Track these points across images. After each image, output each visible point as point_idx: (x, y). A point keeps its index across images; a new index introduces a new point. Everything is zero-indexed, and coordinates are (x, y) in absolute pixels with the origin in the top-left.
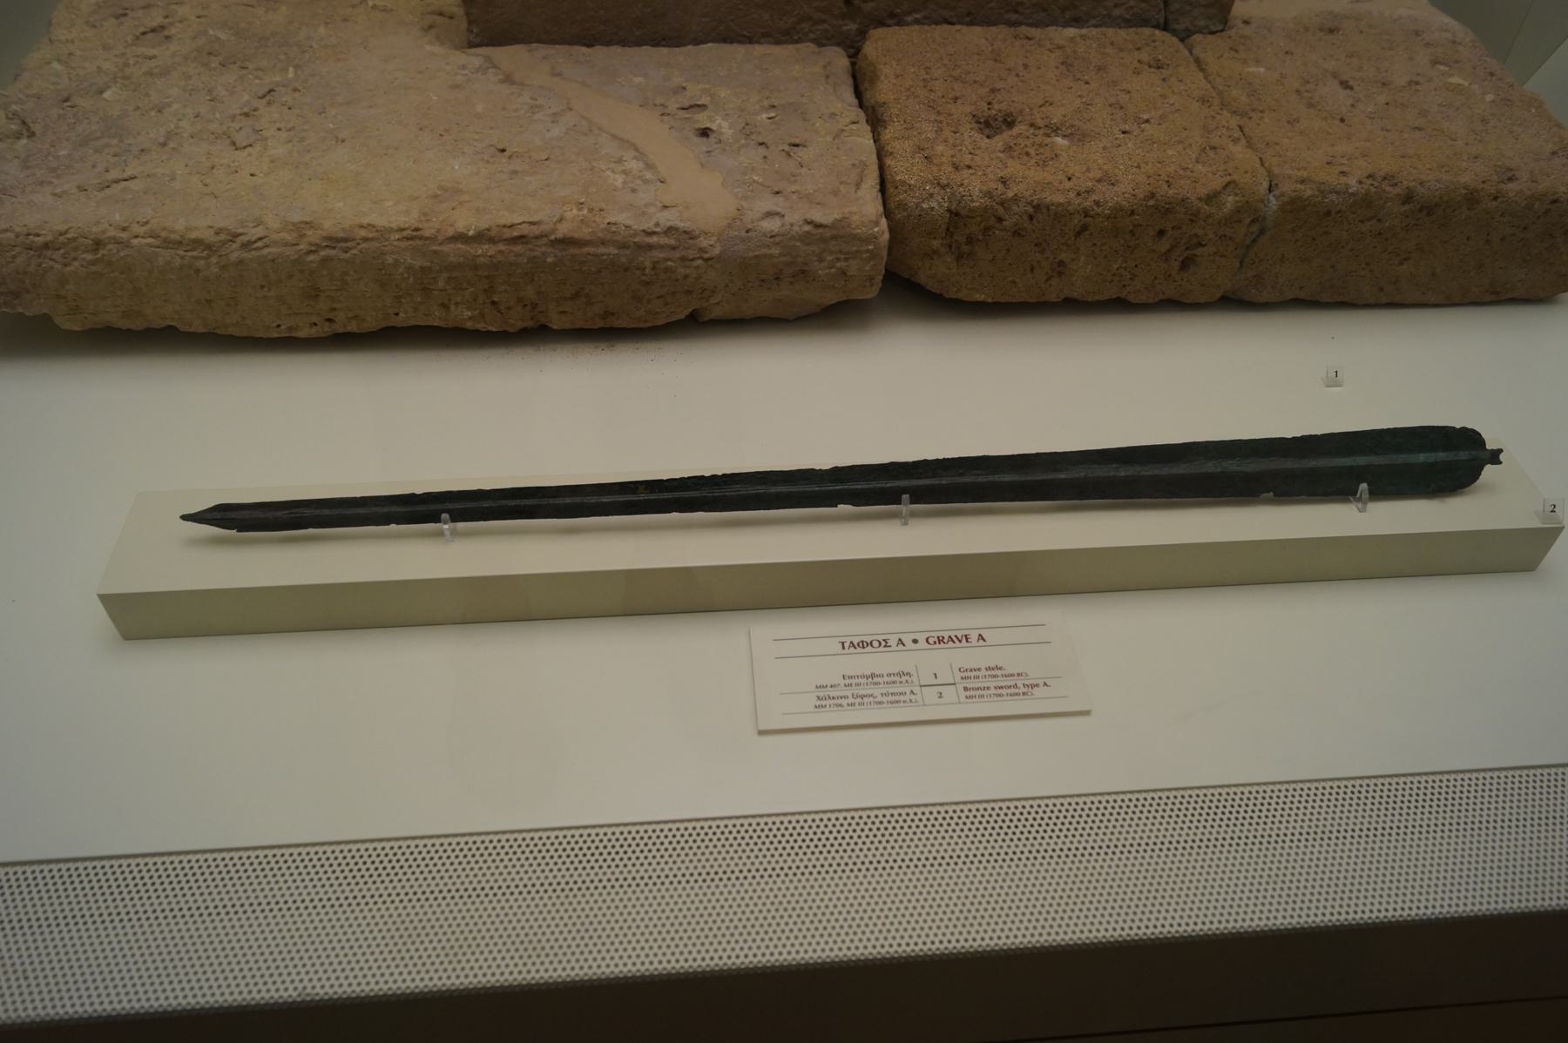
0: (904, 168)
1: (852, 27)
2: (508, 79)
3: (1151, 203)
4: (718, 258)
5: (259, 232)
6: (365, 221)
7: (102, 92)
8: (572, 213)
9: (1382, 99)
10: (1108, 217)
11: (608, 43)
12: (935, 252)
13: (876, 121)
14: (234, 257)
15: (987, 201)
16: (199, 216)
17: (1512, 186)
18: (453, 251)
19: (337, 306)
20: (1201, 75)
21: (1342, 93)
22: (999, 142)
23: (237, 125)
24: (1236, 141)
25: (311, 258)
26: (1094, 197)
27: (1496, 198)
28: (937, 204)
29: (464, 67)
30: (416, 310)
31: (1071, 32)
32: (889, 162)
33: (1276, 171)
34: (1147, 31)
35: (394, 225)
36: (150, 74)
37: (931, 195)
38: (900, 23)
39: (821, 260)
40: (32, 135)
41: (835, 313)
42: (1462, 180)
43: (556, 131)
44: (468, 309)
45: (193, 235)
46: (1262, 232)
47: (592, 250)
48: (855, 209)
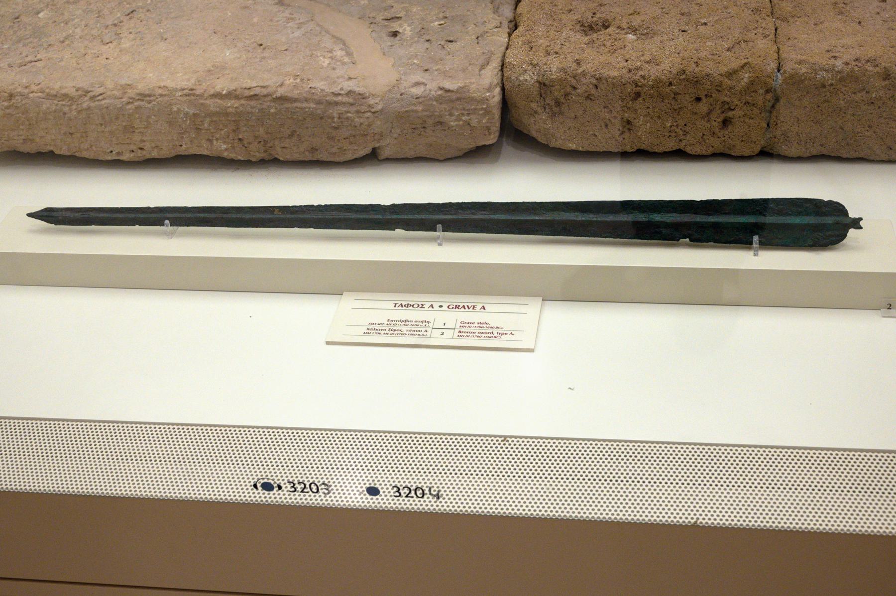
3: (683, 77)
4: (382, 111)
5: (101, 90)
7: (38, 13)
8: (289, 81)
14: (85, 105)
15: (562, 75)
18: (213, 105)
19: (145, 139)
25: (130, 106)
26: (642, 73)
35: (178, 87)
37: (525, 71)
39: (451, 115)
43: (297, 33)
44: (224, 143)
45: (63, 91)
46: (777, 100)
47: (298, 105)
48: (473, 80)
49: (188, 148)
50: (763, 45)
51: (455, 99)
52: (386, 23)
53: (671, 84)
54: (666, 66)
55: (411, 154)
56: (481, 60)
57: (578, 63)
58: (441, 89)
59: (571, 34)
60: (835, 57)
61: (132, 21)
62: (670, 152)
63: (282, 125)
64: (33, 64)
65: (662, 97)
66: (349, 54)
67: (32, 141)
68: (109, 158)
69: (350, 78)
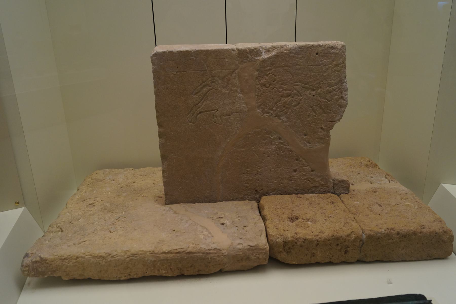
0: (272, 231)
1: (257, 196)
2: (175, 213)
3: (333, 237)
4: (227, 255)
6: (141, 250)
8: (191, 245)
9: (389, 209)
10: (323, 241)
11: (199, 203)
12: (281, 252)
13: (264, 219)
14: (109, 260)
15: (292, 239)
16: (102, 251)
17: (424, 230)
18: (162, 256)
20: (343, 205)
21: (379, 207)
22: (294, 223)
23: (111, 227)
24: (353, 221)
25: (128, 259)
26: (319, 237)
28: (280, 240)
29: (165, 210)
30: (151, 271)
31: (311, 195)
32: (268, 230)
33: (364, 228)
34: (329, 194)
36: (90, 215)
38: (269, 195)
39: (252, 255)
40: (62, 231)
43: (187, 225)
45: (100, 255)
46: (363, 243)
47: (195, 254)
49: (149, 274)
51: (254, 249)
53: (329, 240)
54: (326, 234)
58: (249, 246)
68: (115, 279)
69: (214, 243)
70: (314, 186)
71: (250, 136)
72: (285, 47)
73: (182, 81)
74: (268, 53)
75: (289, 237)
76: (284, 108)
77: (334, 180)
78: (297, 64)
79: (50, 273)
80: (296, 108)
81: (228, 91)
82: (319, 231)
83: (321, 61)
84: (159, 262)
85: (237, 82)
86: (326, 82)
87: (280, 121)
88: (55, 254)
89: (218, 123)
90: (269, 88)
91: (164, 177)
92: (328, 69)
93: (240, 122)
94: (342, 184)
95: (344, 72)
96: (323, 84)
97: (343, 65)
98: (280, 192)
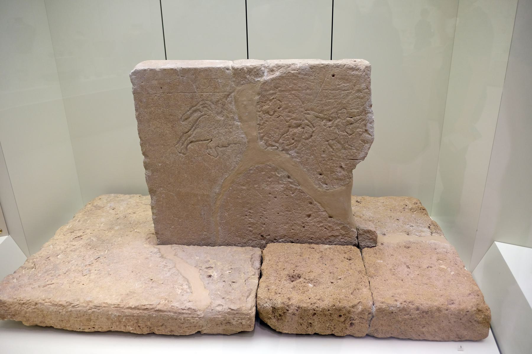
1: (264, 242)
2: (162, 257)
3: (334, 308)
4: (203, 317)
8: (163, 302)
9: (417, 273)
14: (69, 310)
17: (453, 306)
18: (128, 312)
21: (406, 269)
25: (90, 311)
27: (447, 310)
30: (117, 326)
34: (350, 247)
36: (71, 251)
41: (242, 334)
42: (435, 304)
45: (60, 303)
46: (373, 317)
47: (166, 313)
48: (244, 305)
50: (365, 291)
52: (206, 270)
53: (329, 310)
54: (326, 302)
55: (215, 333)
56: (247, 294)
57: (289, 299)
59: (285, 282)
60: (396, 300)
61: (97, 263)
62: (329, 335)
63: (158, 321)
64: (48, 286)
65: (325, 315)
66: (190, 287)
67: (44, 322)
70: (333, 236)
71: (251, 172)
72: (293, 66)
73: (171, 104)
74: (271, 73)
75: (279, 303)
76: (293, 141)
77: (358, 229)
78: (308, 88)
79: (9, 317)
80: (307, 141)
81: (223, 118)
82: (318, 297)
83: (338, 85)
84: (125, 318)
85: (233, 107)
86: (345, 111)
87: (288, 156)
88: (15, 297)
89: (213, 156)
90: (274, 116)
91: (153, 213)
92: (347, 95)
93: (238, 156)
94: (368, 235)
95: (369, 99)
96: (341, 113)
97: (367, 90)
98: (291, 239)
